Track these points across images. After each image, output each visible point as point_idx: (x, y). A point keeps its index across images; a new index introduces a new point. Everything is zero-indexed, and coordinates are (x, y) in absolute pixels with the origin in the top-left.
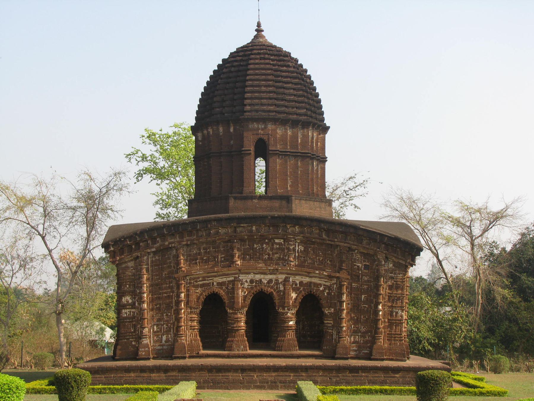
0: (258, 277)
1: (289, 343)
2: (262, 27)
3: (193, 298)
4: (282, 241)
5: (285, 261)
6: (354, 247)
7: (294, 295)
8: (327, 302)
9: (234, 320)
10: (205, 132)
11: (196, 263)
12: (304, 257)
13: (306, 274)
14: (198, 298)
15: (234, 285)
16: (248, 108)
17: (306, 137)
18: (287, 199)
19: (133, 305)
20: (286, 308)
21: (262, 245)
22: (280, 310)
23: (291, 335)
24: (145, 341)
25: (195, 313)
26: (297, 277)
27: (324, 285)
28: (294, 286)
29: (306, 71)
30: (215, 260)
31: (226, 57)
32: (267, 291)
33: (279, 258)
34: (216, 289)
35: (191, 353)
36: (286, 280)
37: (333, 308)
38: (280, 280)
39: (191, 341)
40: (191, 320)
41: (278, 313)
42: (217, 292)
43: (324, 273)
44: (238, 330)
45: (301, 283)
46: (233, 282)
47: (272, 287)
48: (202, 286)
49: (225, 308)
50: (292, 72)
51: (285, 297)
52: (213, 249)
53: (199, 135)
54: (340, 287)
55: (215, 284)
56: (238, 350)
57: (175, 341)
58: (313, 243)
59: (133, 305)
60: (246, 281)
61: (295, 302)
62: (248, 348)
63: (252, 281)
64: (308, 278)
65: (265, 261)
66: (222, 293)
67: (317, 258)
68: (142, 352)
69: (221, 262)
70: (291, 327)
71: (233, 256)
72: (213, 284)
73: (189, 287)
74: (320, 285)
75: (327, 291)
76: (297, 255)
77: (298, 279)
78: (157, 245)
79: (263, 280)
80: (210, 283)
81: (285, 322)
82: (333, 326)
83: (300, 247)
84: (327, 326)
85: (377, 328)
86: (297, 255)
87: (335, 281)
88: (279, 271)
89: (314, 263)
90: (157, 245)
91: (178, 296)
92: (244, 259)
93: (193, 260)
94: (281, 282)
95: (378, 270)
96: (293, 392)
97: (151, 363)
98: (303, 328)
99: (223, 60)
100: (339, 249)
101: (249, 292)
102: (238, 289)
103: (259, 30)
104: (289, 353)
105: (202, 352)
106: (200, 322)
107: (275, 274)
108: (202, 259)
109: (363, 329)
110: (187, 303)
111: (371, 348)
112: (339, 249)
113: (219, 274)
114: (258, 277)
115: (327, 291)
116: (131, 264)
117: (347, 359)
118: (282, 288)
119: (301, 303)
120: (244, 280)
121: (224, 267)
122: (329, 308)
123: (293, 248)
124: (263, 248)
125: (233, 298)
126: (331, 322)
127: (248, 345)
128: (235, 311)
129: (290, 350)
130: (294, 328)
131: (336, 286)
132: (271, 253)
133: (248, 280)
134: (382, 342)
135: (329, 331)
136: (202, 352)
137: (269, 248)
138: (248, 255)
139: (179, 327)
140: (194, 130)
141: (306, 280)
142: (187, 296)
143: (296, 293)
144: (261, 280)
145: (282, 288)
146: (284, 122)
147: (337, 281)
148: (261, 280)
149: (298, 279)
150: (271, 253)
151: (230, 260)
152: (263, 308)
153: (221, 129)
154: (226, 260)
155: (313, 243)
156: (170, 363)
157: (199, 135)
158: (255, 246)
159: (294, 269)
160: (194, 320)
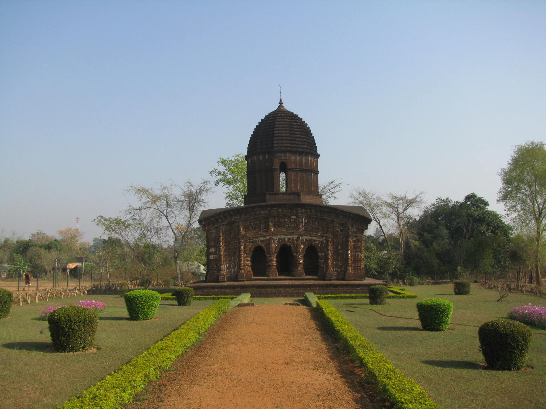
0: (282, 237)
2: (282, 102)
3: (248, 249)
4: (295, 217)
5: (297, 228)
6: (334, 220)
7: (302, 246)
10: (253, 159)
14: (250, 249)
16: (276, 145)
17: (307, 160)
18: (298, 194)
19: (215, 253)
22: (295, 255)
23: (301, 268)
24: (222, 272)
25: (249, 257)
29: (307, 125)
31: (263, 118)
33: (294, 227)
34: (260, 244)
36: (298, 238)
45: (306, 240)
46: (269, 240)
47: (290, 242)
48: (252, 242)
50: (300, 125)
53: (249, 160)
54: (328, 241)
57: (238, 272)
58: (313, 218)
59: (215, 253)
63: (279, 239)
65: (286, 228)
66: (263, 246)
68: (221, 278)
71: (269, 226)
74: (317, 241)
77: (304, 238)
78: (228, 220)
85: (348, 264)
87: (324, 238)
90: (228, 220)
91: (240, 248)
92: (275, 227)
95: (348, 232)
96: (303, 298)
97: (226, 284)
99: (262, 120)
103: (281, 103)
105: (253, 277)
106: (252, 262)
109: (340, 264)
110: (244, 252)
111: (344, 274)
114: (282, 237)
116: (214, 231)
117: (332, 280)
118: (296, 243)
119: (306, 251)
121: (264, 232)
134: (350, 270)
136: (253, 277)
139: (240, 265)
140: (247, 157)
141: (309, 238)
142: (244, 248)
144: (284, 239)
145: (296, 243)
146: (295, 153)
149: (304, 238)
152: (286, 255)
153: (261, 157)
155: (313, 218)
156: (236, 283)
157: (249, 160)
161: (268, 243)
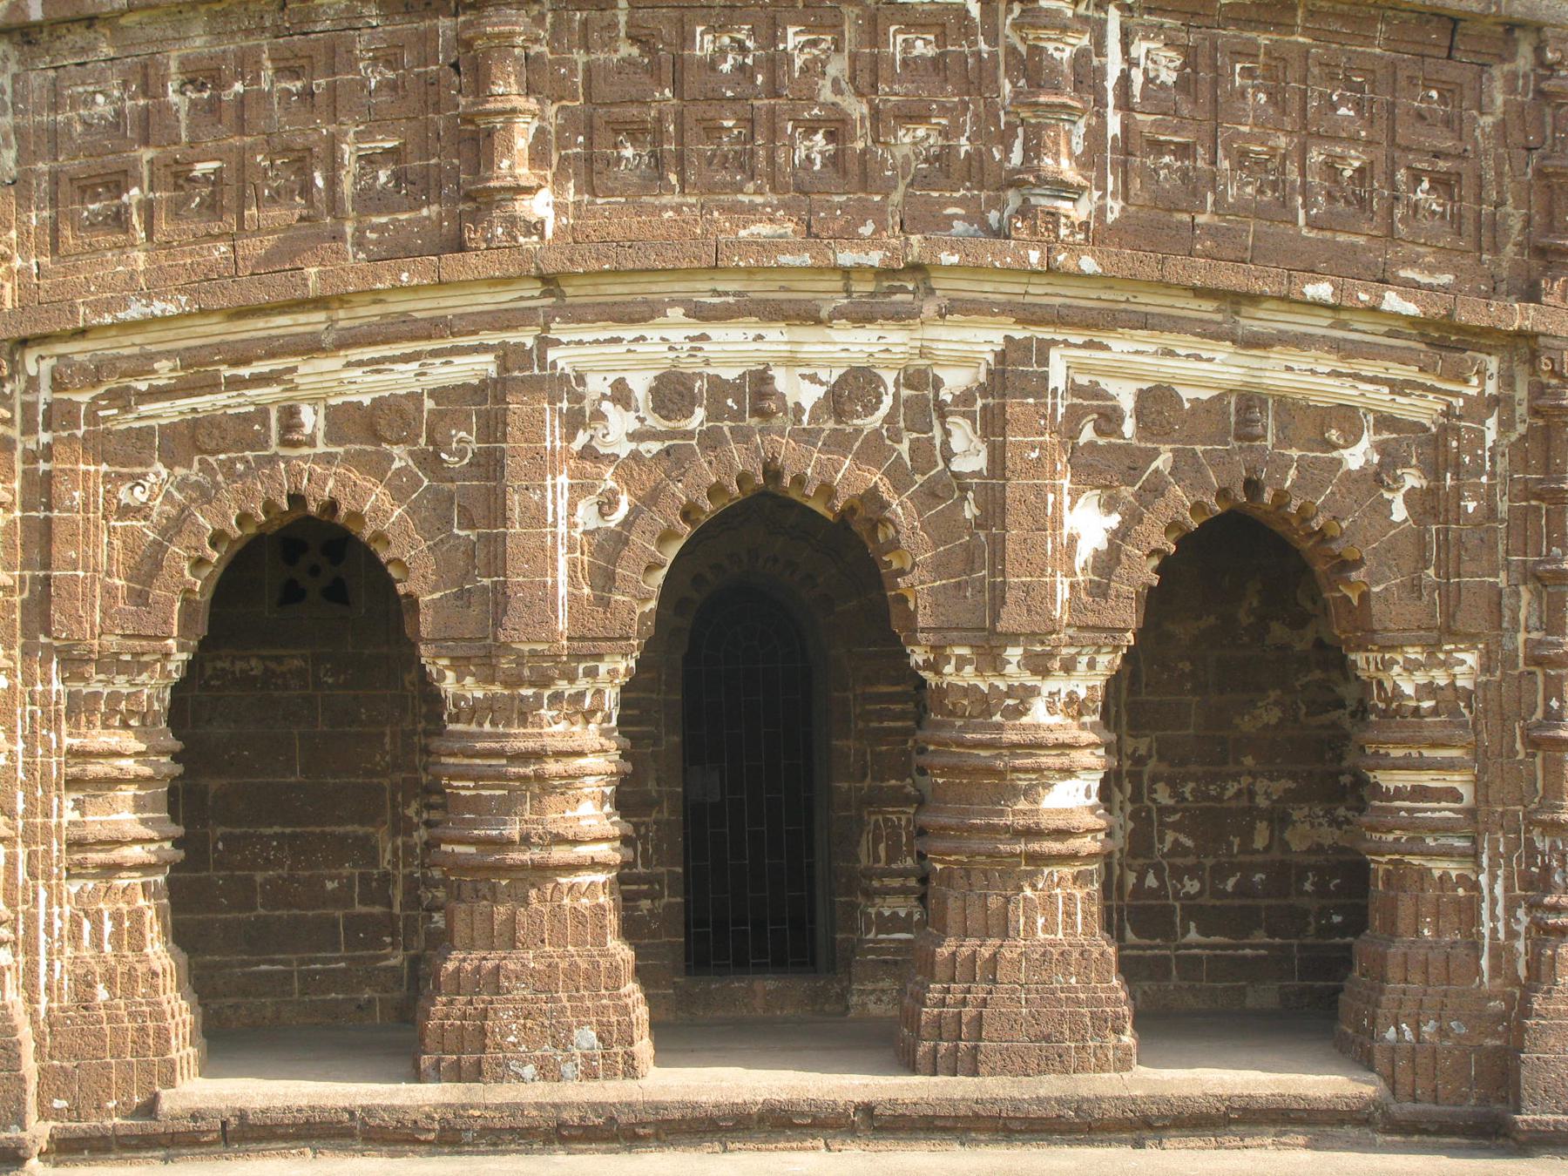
0: (732, 348)
1: (1049, 997)
5: (995, 184)
7: (1088, 524)
8: (1415, 587)
9: (500, 777)
11: (119, 220)
12: (1184, 151)
13: (1206, 309)
14: (147, 567)
15: (494, 427)
20: (1014, 653)
21: (771, 34)
23: (1058, 921)
25: (118, 714)
26: (1122, 346)
27: (1385, 422)
28: (1087, 434)
30: (307, 189)
32: (827, 491)
33: (942, 160)
34: (325, 476)
35: (75, 1112)
37: (1471, 639)
38: (955, 381)
39: (85, 983)
40: (74, 783)
41: (919, 697)
42: (332, 506)
43: (1392, 301)
44: (544, 871)
45: (1157, 402)
47: (873, 449)
48: (186, 441)
49: (413, 661)
51: (998, 546)
52: (280, 72)
55: (311, 419)
56: (548, 1072)
60: (621, 395)
61: (1099, 590)
62: (644, 1046)
63: (672, 393)
64: (1223, 352)
65: (799, 190)
66: (380, 507)
67: (1316, 156)
69: (369, 201)
70: (1062, 834)
71: (479, 142)
72: (290, 417)
73: (48, 452)
74: (1348, 419)
75: (1412, 480)
76: (1114, 125)
77: (1127, 364)
79: (782, 380)
80: (262, 413)
81: (1001, 786)
82: (1474, 821)
83: (1139, 49)
84: (1412, 825)
86: (1114, 125)
87: (1486, 377)
88: (941, 283)
89: (1284, 203)
92: (591, 172)
93: (86, 189)
94: (965, 398)
98: (1139, 844)
100: (1524, 60)
101: (649, 500)
102: (541, 464)
104: (1052, 1086)
106: (186, 801)
107: (901, 316)
108: (180, 177)
112: (1524, 60)
113: (344, 318)
114: (732, 348)
115: (1412, 480)
118: (968, 453)
119: (1156, 603)
120: (597, 385)
121: (398, 250)
122: (1432, 647)
123: (1081, 56)
124: (775, 63)
125: (494, 554)
126: (1459, 781)
127: (642, 1013)
128: (515, 681)
129: (1059, 1063)
130: (1088, 845)
131: (1505, 426)
132: (857, 109)
133: (640, 384)
135: (1438, 867)
137: (838, 67)
138: (635, 132)
141: (1208, 370)
143: (1109, 506)
144: (760, 381)
147: (1508, 380)
148: (760, 381)
149: (1127, 364)
150: (857, 109)
151: (452, 181)
154: (414, 186)
158: (704, 44)
159: (1088, 264)
160: (112, 782)
161: (476, 452)
